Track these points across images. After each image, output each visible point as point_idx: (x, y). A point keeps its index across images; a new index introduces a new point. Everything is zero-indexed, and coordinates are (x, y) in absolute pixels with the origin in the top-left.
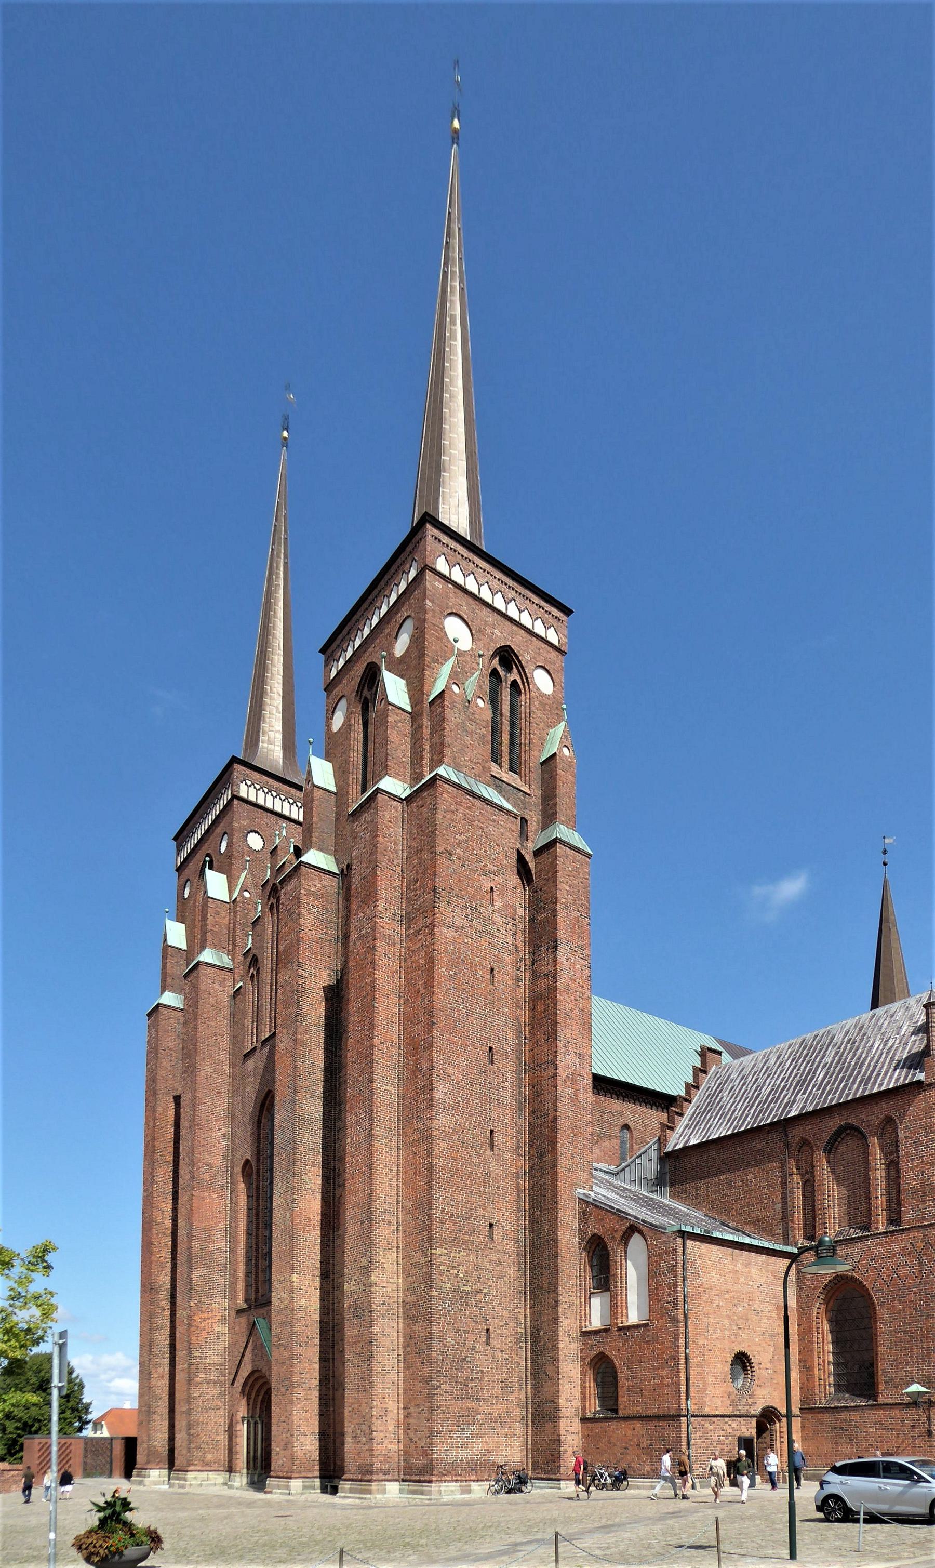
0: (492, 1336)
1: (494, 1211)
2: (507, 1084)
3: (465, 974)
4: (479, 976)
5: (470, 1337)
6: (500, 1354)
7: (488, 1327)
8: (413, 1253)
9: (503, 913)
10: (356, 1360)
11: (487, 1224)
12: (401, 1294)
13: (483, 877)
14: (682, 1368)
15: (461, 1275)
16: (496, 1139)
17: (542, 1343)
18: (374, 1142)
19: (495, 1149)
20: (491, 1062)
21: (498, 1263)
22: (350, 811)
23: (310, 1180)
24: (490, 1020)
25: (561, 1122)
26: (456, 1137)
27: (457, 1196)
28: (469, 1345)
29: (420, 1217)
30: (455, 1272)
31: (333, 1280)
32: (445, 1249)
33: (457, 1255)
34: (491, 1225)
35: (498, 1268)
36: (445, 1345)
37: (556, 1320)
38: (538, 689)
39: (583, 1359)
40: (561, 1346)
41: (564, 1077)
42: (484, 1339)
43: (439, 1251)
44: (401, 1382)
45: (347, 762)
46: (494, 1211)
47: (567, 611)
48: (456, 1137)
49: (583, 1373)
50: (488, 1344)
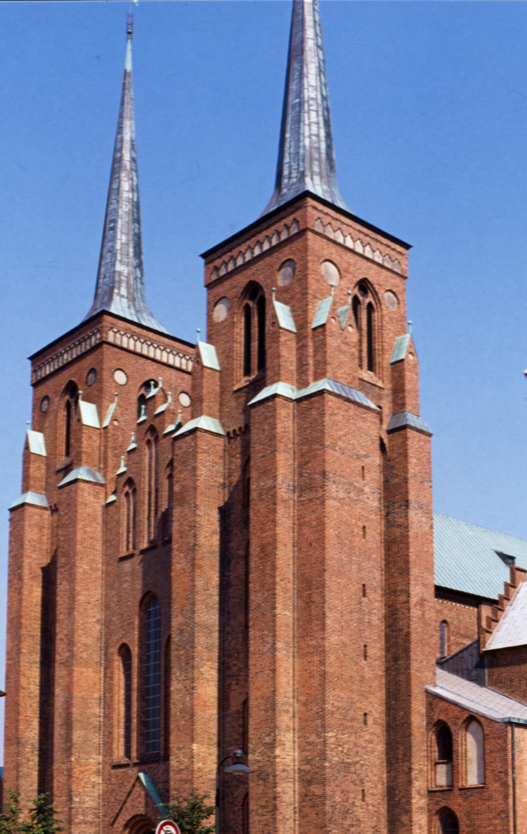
12: (297, 763)
14: (511, 819)
15: (345, 751)
17: (397, 799)
19: (368, 658)
20: (364, 595)
22: (235, 388)
27: (342, 695)
36: (334, 802)
37: (410, 782)
39: (429, 811)
40: (414, 801)
43: (330, 734)
44: (297, 828)
45: (231, 350)
49: (430, 821)
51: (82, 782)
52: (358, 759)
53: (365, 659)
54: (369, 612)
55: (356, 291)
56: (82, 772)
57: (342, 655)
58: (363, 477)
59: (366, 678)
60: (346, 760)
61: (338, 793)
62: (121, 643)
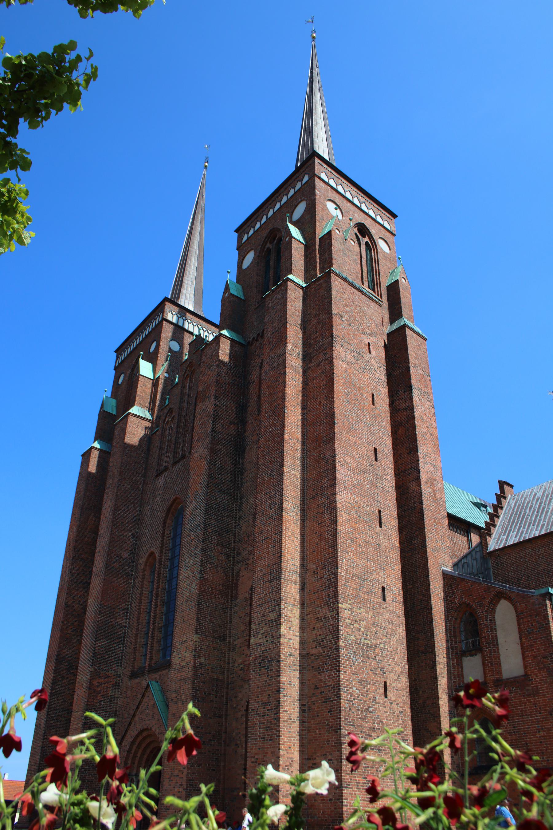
0: (388, 688)
1: (385, 576)
2: (388, 477)
3: (355, 394)
4: (364, 397)
5: (372, 688)
6: (395, 707)
7: (385, 680)
8: (318, 609)
9: (377, 360)
10: (261, 710)
11: (380, 586)
13: (362, 335)
15: (362, 629)
16: (382, 518)
18: (284, 513)
19: (383, 526)
20: (376, 460)
21: (391, 622)
23: (215, 556)
24: (374, 429)
25: (426, 512)
26: (354, 512)
27: (357, 560)
28: (371, 695)
29: (326, 576)
30: (358, 626)
31: (229, 642)
32: (350, 604)
33: (359, 611)
34: (383, 589)
35: (390, 626)
36: (351, 694)
38: (382, 249)
41: (425, 480)
42: (382, 691)
46: (385, 576)
47: (395, 216)
48: (354, 512)
50: (386, 696)
51: (100, 695)
52: (377, 641)
53: (381, 526)
54: (382, 476)
55: (356, 230)
56: (101, 684)
57: (355, 516)
58: (370, 352)
59: (382, 546)
60: (363, 641)
61: (355, 683)
62: (149, 552)
